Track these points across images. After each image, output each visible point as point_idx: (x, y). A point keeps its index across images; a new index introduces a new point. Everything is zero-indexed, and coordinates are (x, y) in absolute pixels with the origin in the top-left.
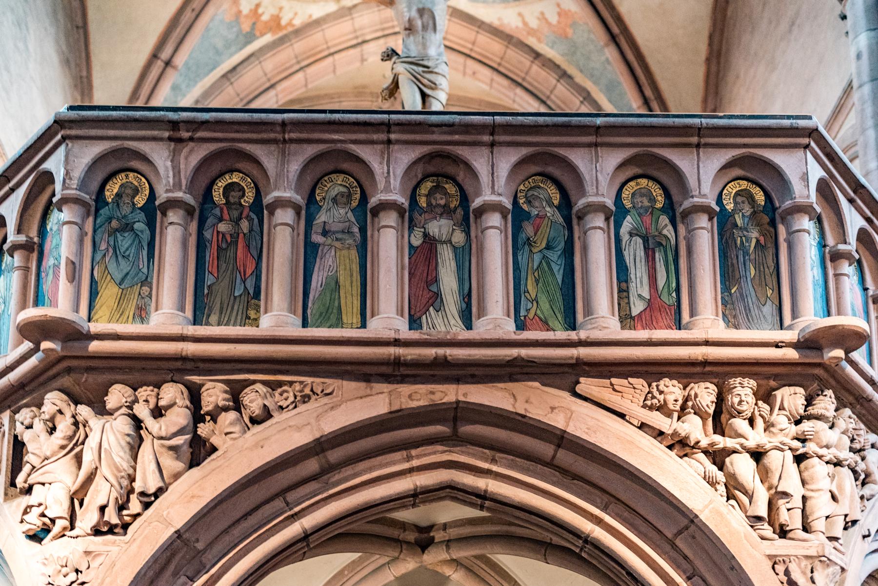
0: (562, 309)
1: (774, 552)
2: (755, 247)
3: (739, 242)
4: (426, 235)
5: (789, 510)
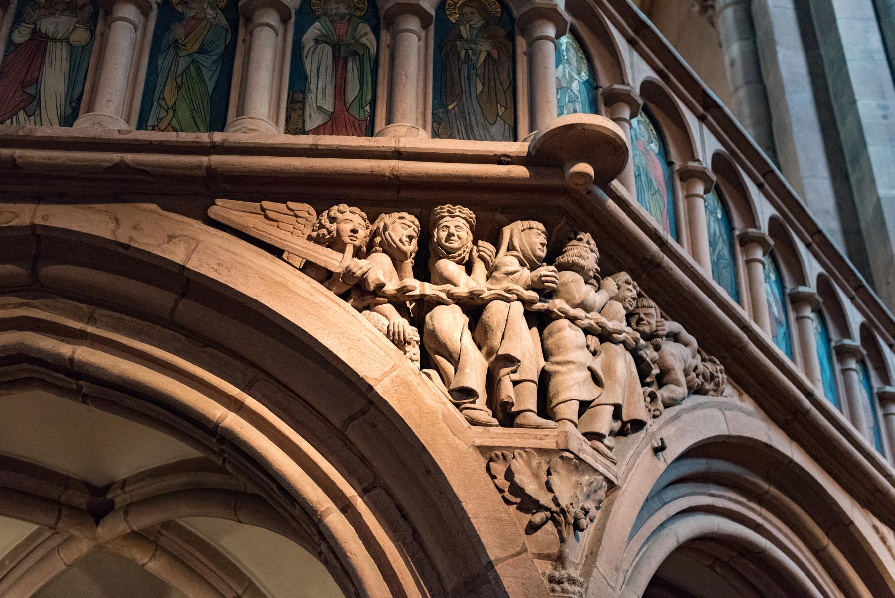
0: (208, 119)
1: (488, 442)
2: (485, 61)
4: (35, 32)
5: (515, 383)
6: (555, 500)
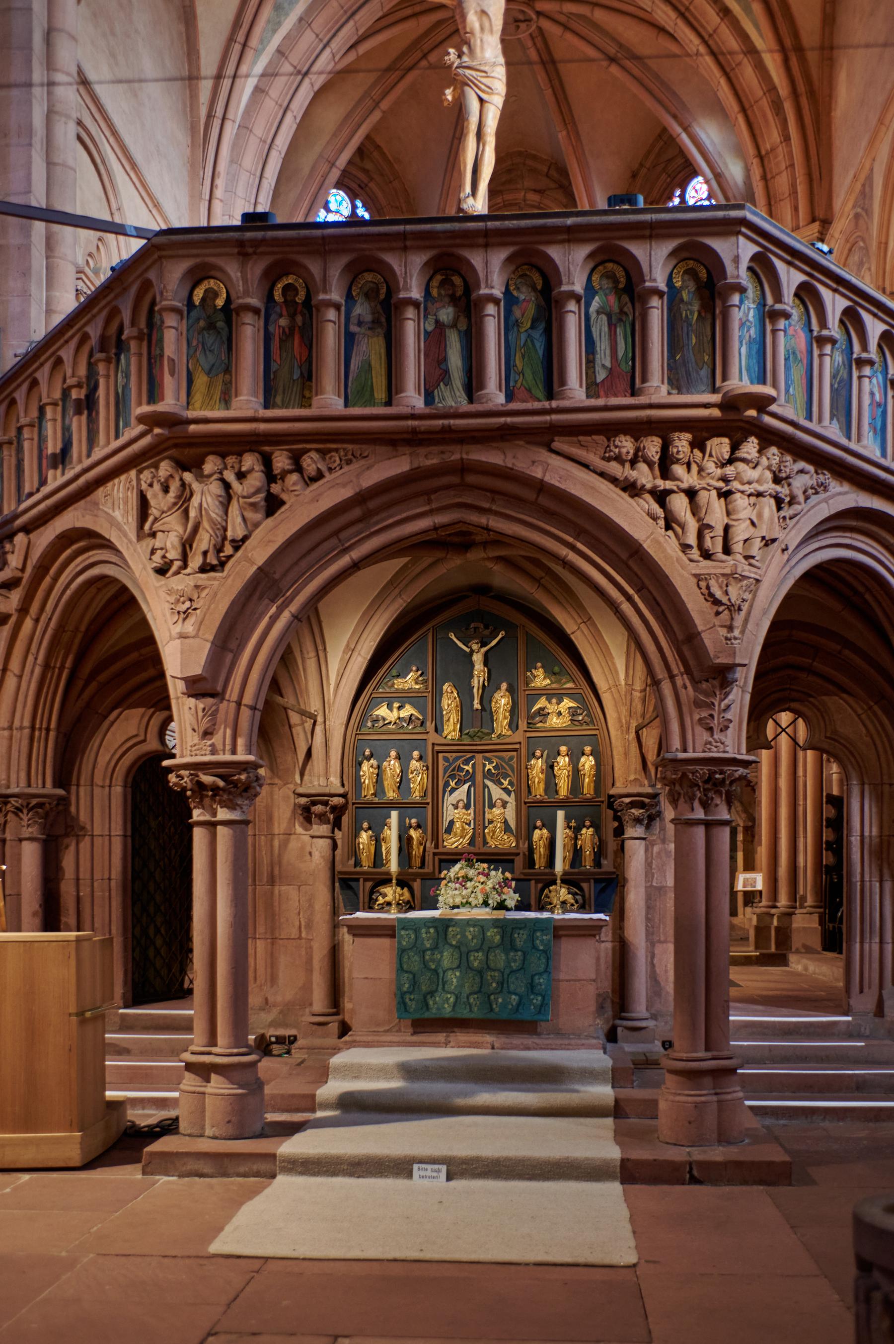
1: (698, 572)
3: (684, 315)
4: (437, 322)
5: (712, 538)
6: (729, 600)
